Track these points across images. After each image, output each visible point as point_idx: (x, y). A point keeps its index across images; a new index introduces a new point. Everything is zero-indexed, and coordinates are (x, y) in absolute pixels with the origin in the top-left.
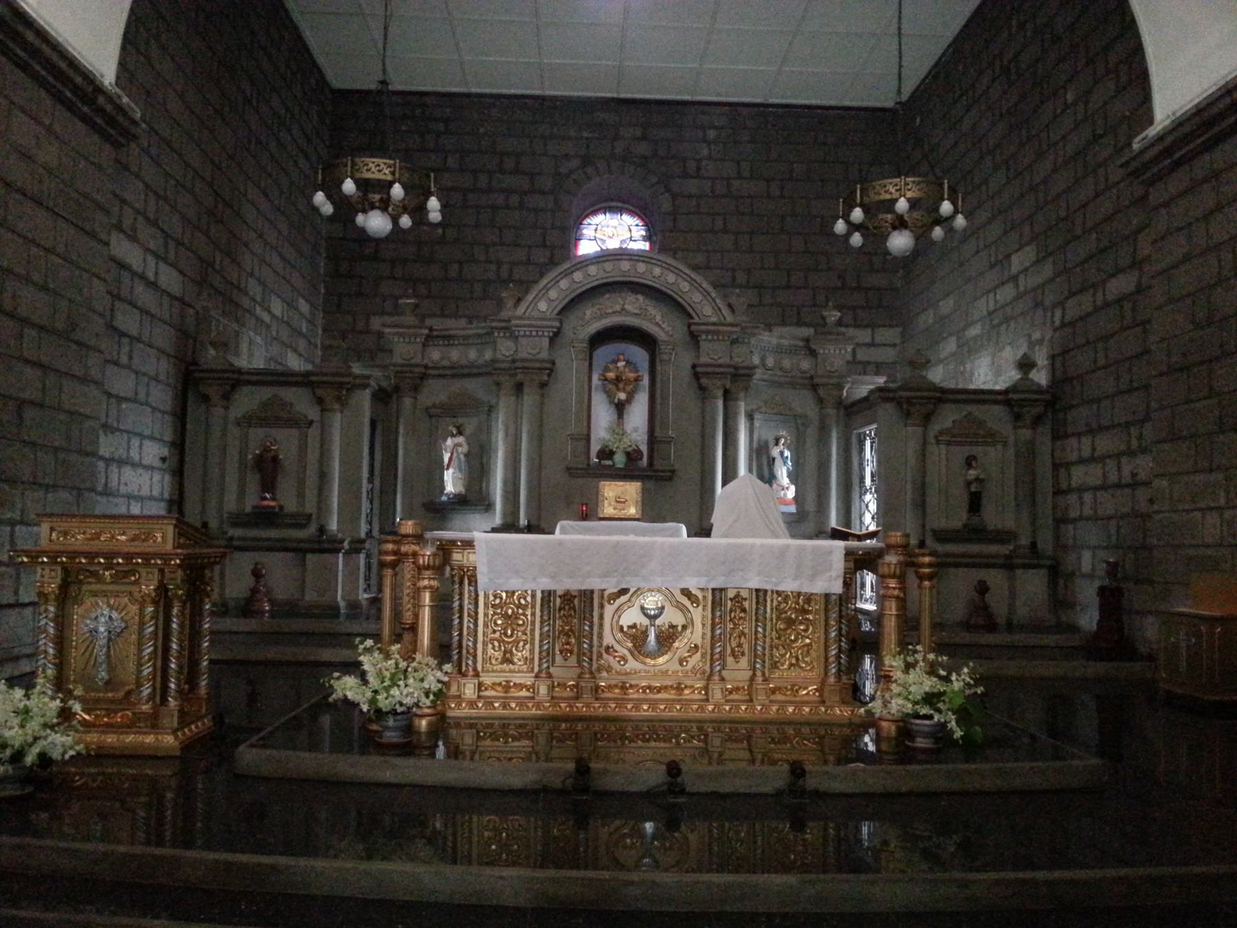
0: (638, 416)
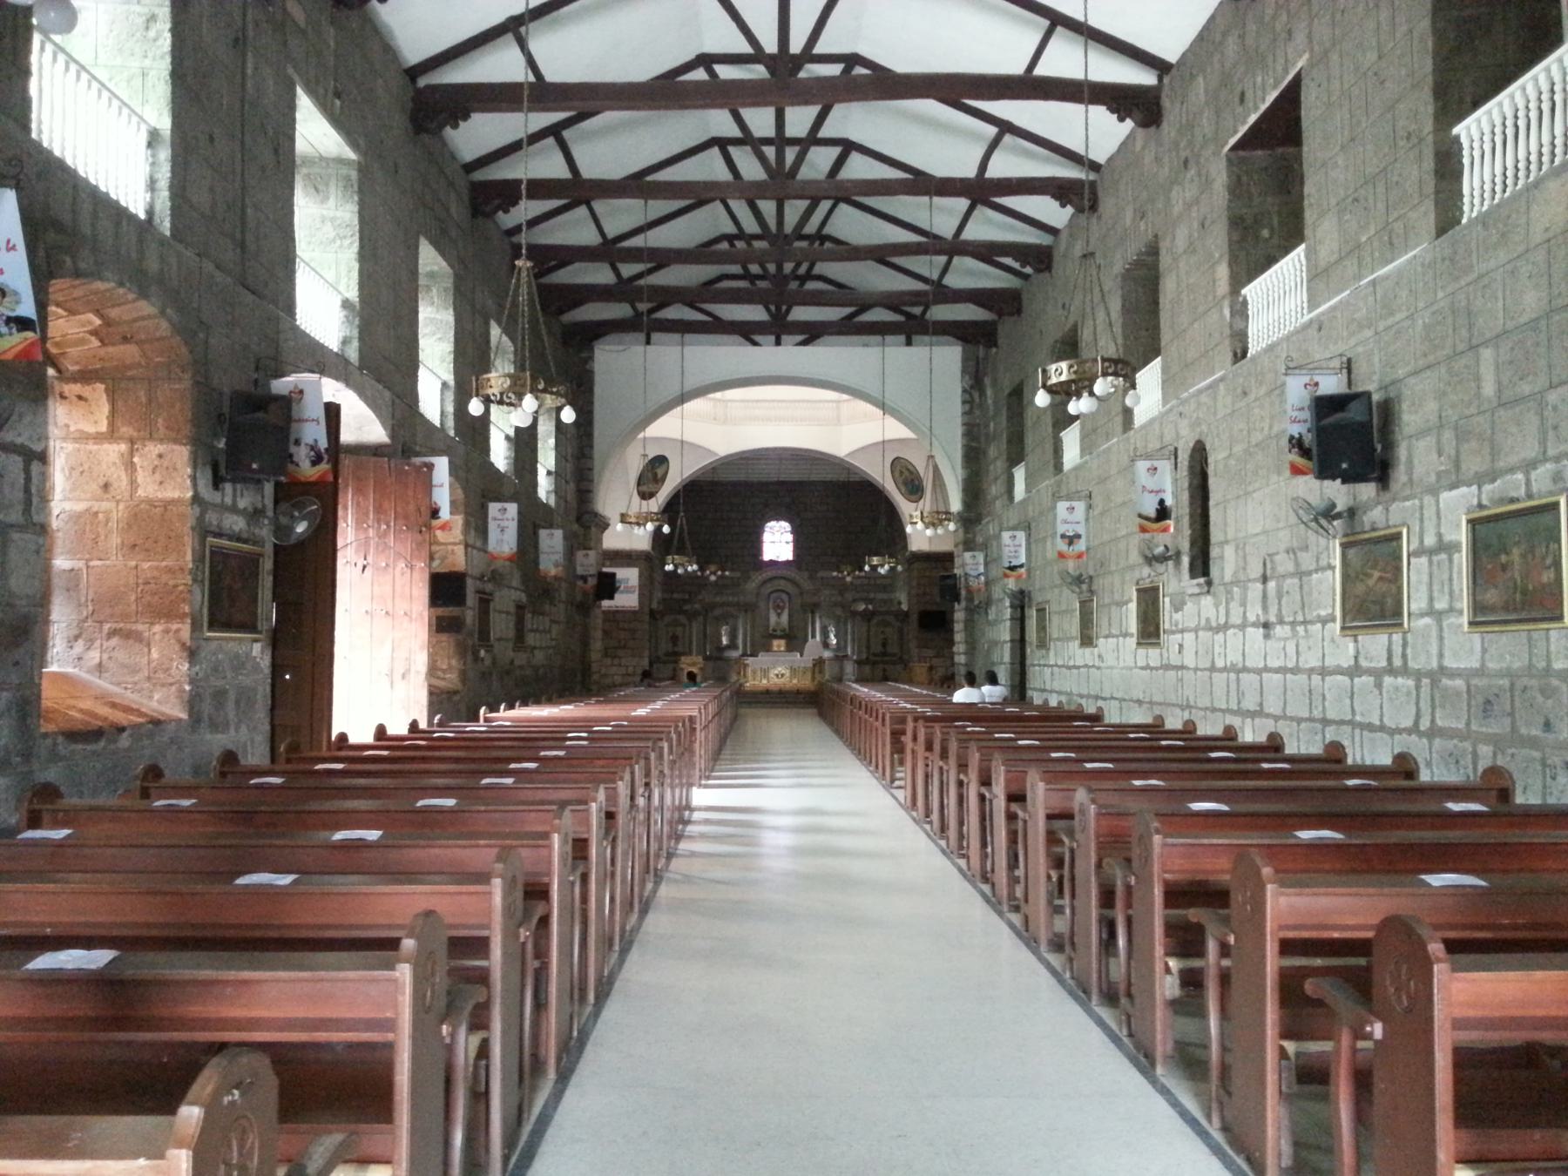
0: (785, 618)
